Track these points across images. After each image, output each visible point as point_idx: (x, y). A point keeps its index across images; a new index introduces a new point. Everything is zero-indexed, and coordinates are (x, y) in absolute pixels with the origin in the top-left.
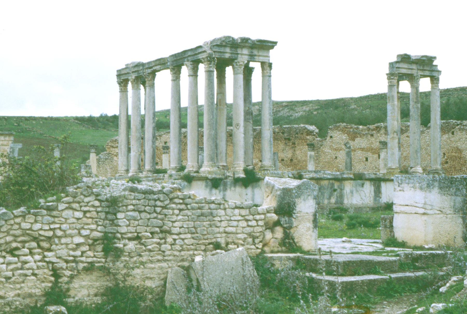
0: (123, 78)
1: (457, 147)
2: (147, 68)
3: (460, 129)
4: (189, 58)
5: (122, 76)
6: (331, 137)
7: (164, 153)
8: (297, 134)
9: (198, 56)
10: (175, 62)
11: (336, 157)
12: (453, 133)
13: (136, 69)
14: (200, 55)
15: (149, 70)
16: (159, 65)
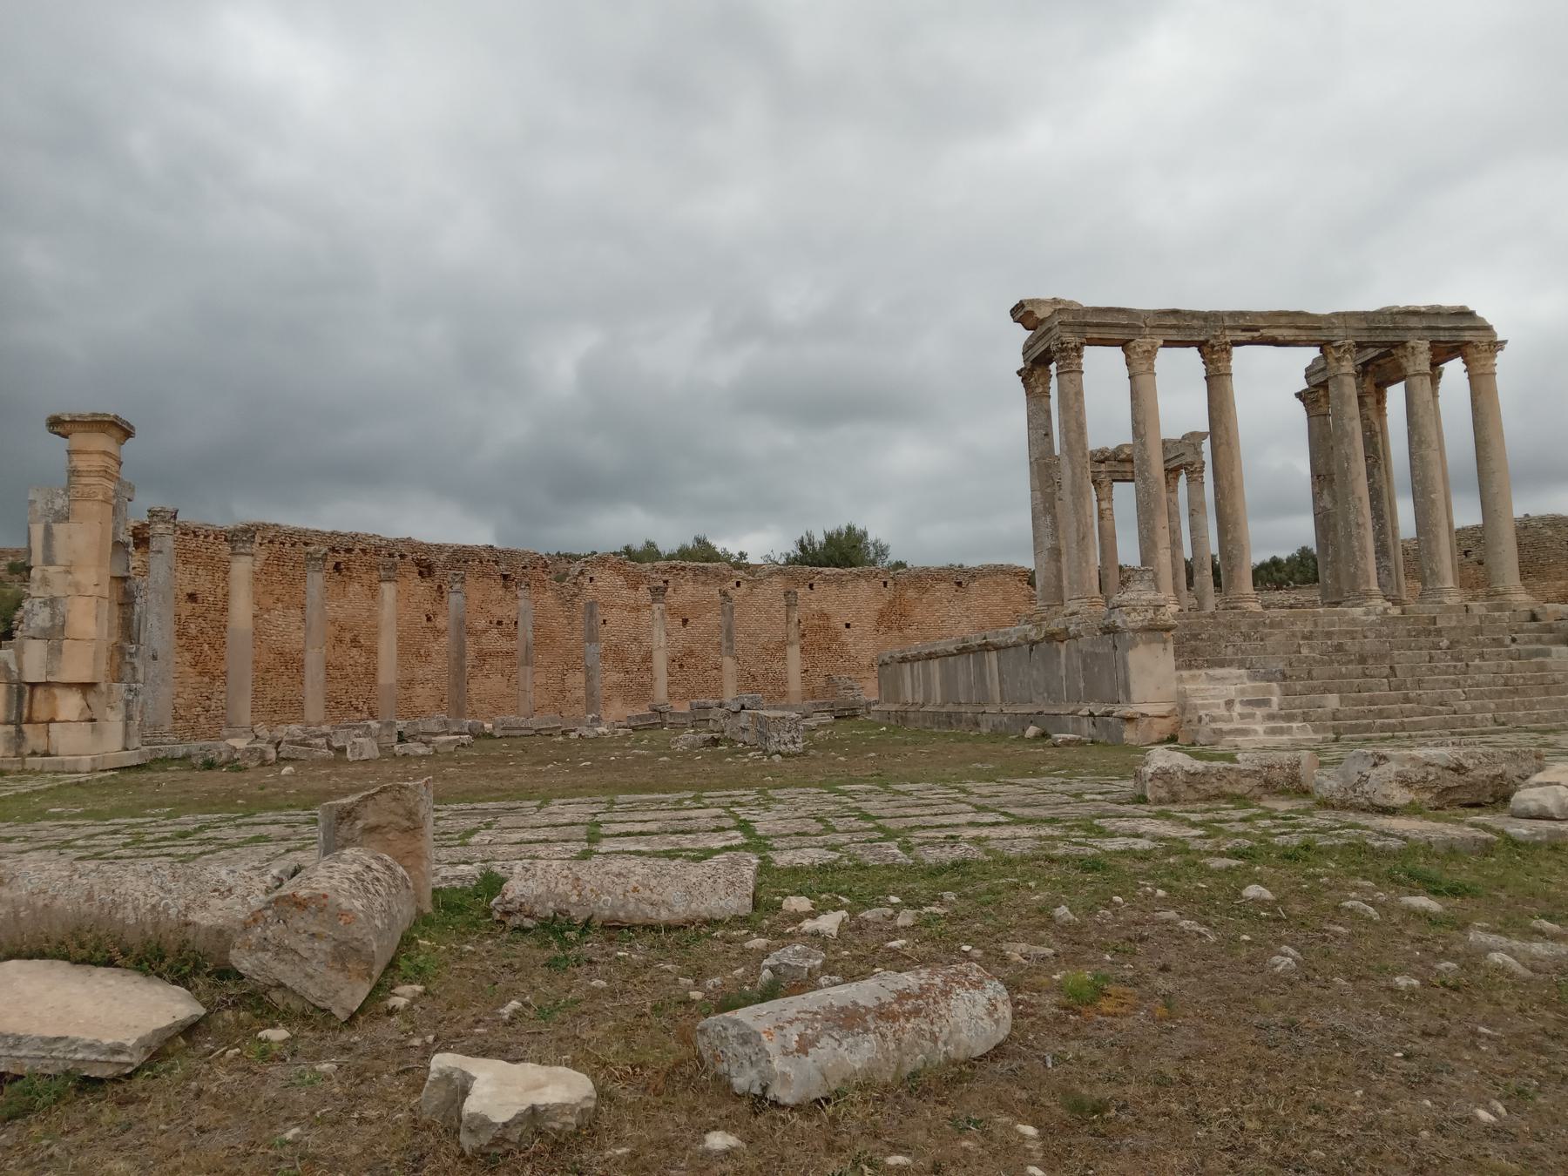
0: (1089, 336)
1: (821, 610)
2: (1232, 328)
3: (825, 581)
4: (1426, 333)
5: (1088, 329)
6: (591, 579)
7: (389, 580)
8: (525, 568)
9: (1462, 333)
10: (1365, 333)
11: (605, 621)
12: (811, 586)
13: (1172, 321)
14: (1467, 333)
15: (1239, 333)
16: (1290, 327)
